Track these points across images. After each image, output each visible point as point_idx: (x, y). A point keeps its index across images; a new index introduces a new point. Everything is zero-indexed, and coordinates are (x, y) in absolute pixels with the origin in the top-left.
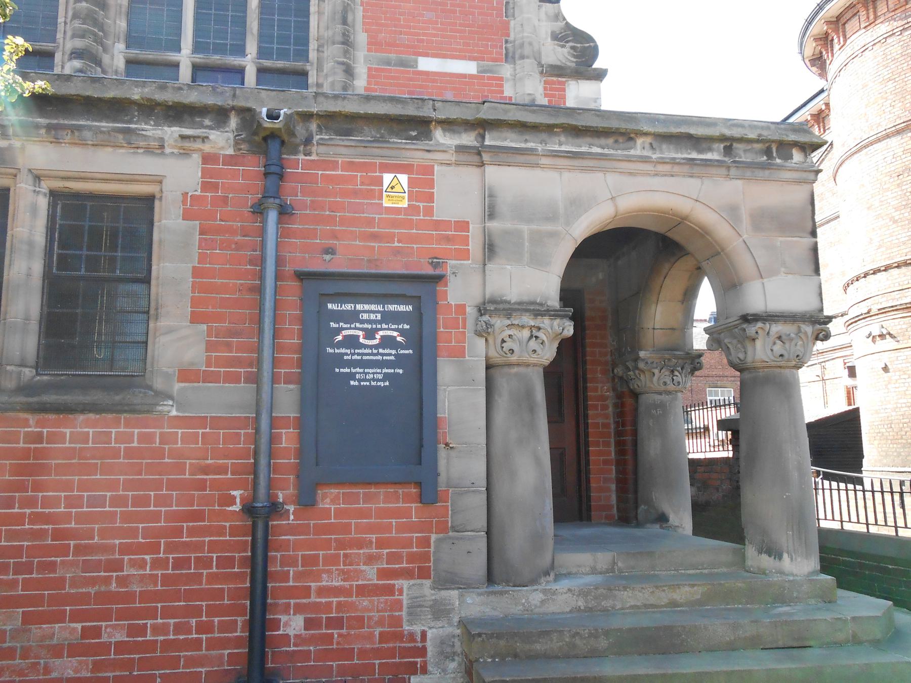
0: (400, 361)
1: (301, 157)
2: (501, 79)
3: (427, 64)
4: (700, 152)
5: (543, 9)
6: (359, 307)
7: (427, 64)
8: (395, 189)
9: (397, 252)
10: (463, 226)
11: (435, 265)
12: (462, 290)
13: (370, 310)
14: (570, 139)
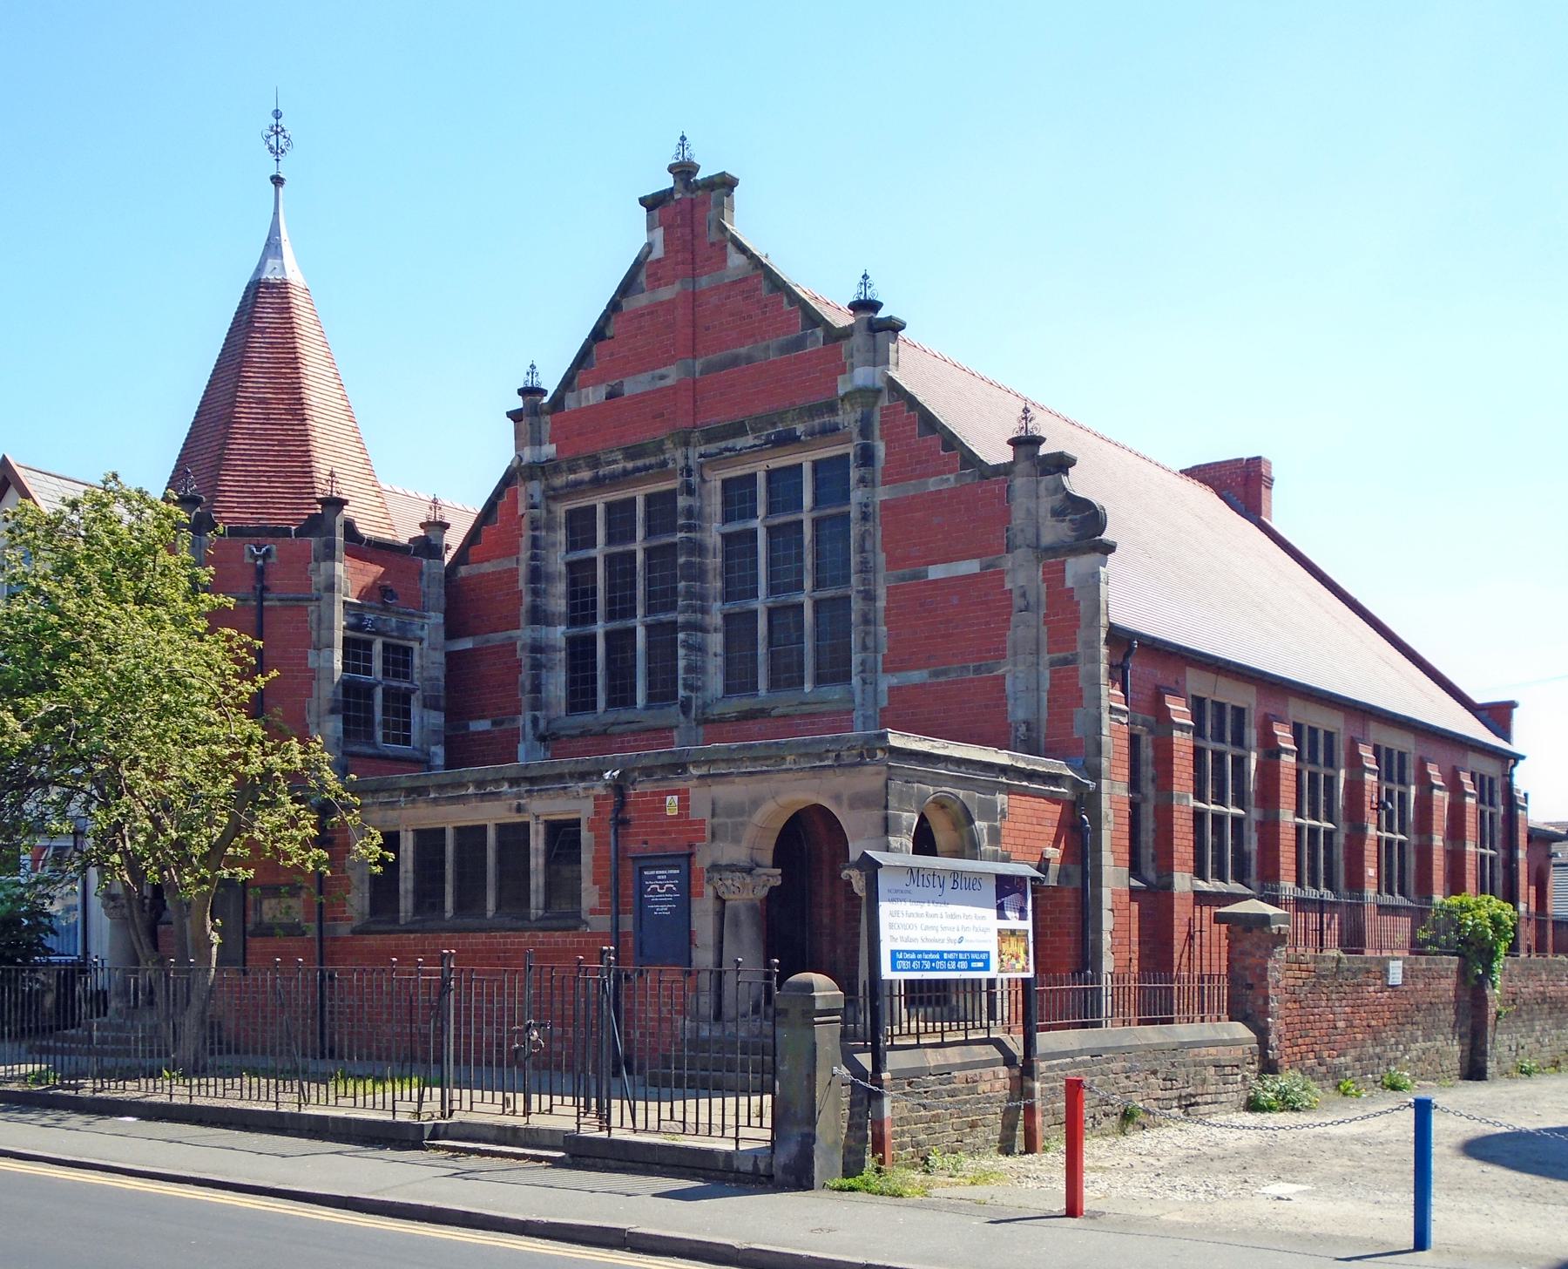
0: (675, 900)
2: (1002, 572)
3: (936, 572)
5: (1042, 486)
7: (936, 572)
8: (672, 801)
12: (703, 860)
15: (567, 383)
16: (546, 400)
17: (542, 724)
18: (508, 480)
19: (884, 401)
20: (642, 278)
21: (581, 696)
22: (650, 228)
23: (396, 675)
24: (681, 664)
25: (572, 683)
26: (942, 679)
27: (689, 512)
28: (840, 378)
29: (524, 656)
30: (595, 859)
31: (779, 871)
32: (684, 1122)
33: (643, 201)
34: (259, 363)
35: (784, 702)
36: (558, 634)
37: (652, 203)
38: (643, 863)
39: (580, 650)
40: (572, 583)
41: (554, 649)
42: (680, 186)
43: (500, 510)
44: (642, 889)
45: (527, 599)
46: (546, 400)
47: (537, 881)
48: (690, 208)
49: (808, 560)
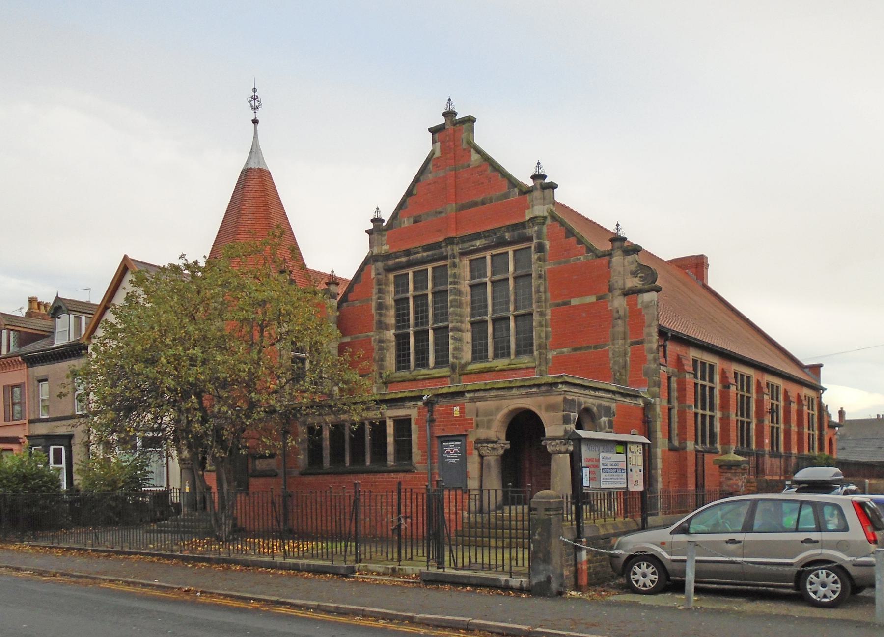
3: (574, 302)
7: (574, 302)
8: (457, 410)
10: (472, 419)
13: (451, 444)
15: (394, 216)
16: (384, 224)
17: (384, 375)
18: (366, 262)
19: (549, 221)
20: (430, 166)
21: (402, 361)
22: (434, 142)
24: (451, 347)
25: (398, 357)
26: (578, 352)
27: (455, 276)
28: (527, 212)
29: (376, 346)
30: (419, 438)
32: (483, 564)
33: (430, 130)
34: (255, 201)
35: (501, 363)
36: (390, 334)
37: (434, 131)
39: (402, 341)
40: (397, 310)
41: (390, 341)
42: (449, 122)
43: (363, 276)
44: (443, 452)
45: (376, 318)
46: (384, 224)
47: (390, 449)
48: (453, 132)
49: (512, 298)
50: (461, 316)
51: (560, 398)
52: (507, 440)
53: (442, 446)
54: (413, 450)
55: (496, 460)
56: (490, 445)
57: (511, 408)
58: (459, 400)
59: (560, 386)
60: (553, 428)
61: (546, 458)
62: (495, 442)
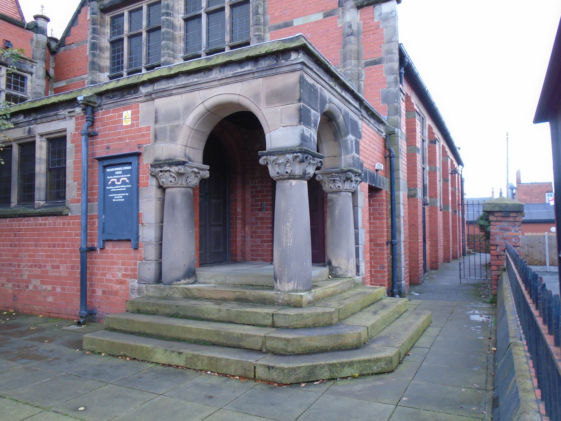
0: (128, 190)
1: (100, 111)
4: (242, 68)
6: (116, 169)
9: (127, 144)
10: (148, 128)
11: (139, 148)
13: (118, 170)
14: (186, 78)
23: (16, 89)
30: (75, 163)
31: (208, 167)
38: (106, 163)
40: (113, 52)
44: (105, 183)
45: (90, 59)
49: (228, 27)
50: (173, 50)
51: (294, 78)
52: (204, 163)
53: (104, 172)
54: (68, 182)
55: (186, 194)
56: (174, 169)
57: (209, 103)
58: (130, 99)
59: (294, 56)
60: (282, 132)
61: (266, 188)
62: (183, 163)
